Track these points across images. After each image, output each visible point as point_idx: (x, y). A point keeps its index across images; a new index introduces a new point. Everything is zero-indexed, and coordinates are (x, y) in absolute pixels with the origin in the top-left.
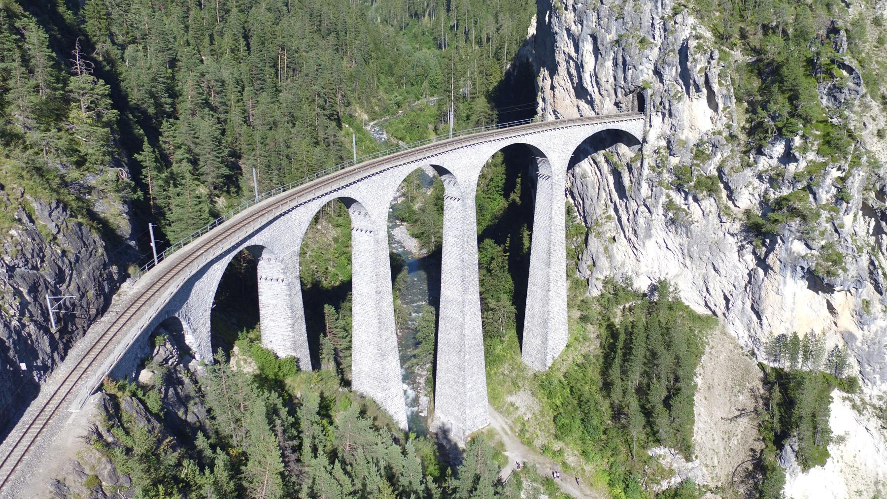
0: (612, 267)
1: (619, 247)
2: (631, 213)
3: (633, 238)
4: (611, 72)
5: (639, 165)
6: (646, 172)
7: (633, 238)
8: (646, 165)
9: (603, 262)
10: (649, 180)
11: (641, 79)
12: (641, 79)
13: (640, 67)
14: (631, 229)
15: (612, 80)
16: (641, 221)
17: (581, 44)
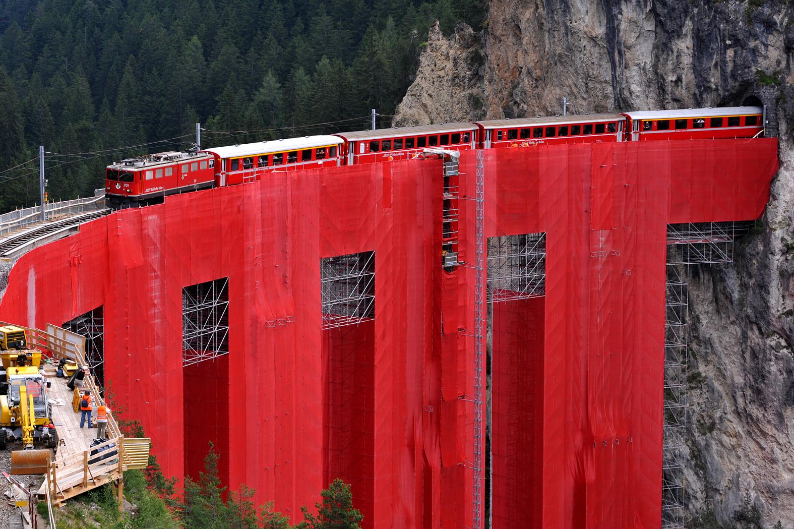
0: (710, 489)
1: (726, 439)
2: (748, 355)
3: (756, 411)
4: (687, 60)
5: (761, 247)
6: (777, 260)
7: (756, 411)
8: (777, 245)
9: (690, 480)
10: (783, 274)
11: (754, 69)
12: (754, 69)
13: (752, 44)
14: (749, 392)
15: (688, 77)
16: (774, 369)
17: (615, 11)
